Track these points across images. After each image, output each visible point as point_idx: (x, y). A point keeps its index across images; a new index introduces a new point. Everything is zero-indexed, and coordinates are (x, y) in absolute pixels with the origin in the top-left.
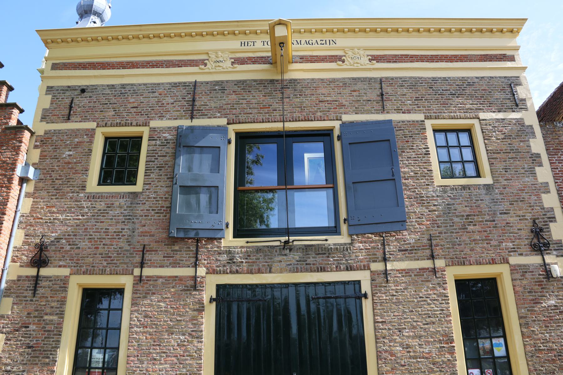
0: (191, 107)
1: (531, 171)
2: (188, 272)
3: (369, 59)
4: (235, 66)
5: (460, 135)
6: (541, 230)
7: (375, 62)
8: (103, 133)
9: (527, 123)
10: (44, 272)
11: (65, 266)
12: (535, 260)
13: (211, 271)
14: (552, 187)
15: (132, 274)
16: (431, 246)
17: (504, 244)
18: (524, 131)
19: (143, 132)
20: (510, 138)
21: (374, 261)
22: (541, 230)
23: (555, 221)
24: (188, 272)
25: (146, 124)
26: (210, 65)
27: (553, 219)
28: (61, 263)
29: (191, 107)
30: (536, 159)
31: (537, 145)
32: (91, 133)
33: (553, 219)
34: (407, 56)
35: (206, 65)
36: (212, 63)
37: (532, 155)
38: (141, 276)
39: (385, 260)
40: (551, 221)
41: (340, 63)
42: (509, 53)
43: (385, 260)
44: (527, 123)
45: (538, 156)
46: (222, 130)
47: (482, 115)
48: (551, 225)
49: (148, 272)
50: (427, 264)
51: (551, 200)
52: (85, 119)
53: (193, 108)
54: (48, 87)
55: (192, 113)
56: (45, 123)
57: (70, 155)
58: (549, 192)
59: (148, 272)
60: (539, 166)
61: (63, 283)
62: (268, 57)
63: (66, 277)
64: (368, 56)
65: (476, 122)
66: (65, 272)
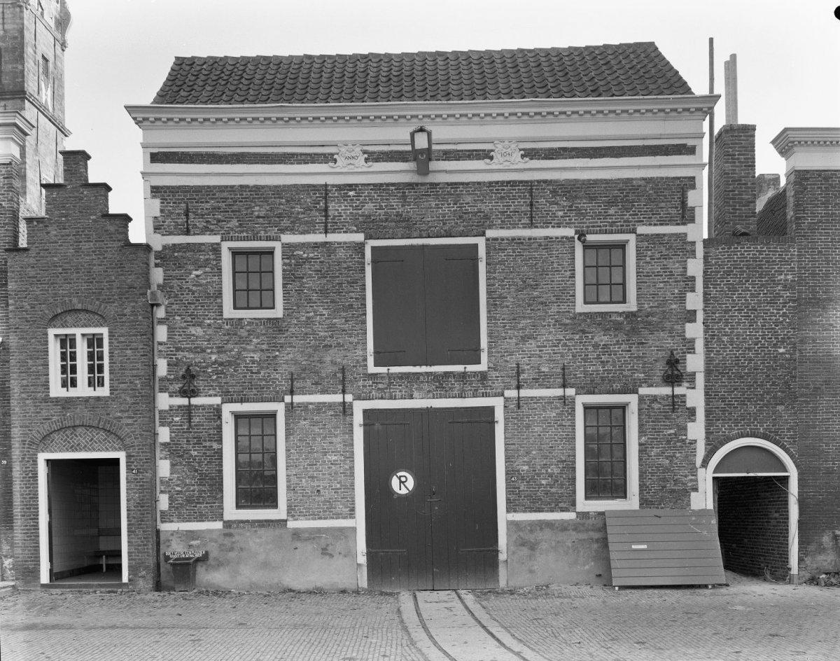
0: (324, 218)
1: (680, 297)
2: (338, 398)
3: (522, 155)
4: (370, 163)
5: (612, 253)
6: (677, 361)
7: (527, 159)
8: (230, 249)
9: (689, 239)
10: (195, 401)
11: (215, 395)
12: (666, 391)
13: (358, 398)
14: (700, 316)
15: (283, 401)
16: (564, 375)
17: (636, 375)
18: (684, 247)
19: (274, 248)
20: (666, 259)
21: (508, 389)
22: (677, 361)
23: (694, 353)
24: (338, 398)
25: (277, 239)
26: (341, 161)
27: (692, 350)
28: (211, 392)
29: (324, 218)
30: (689, 283)
31: (695, 267)
32: (216, 249)
33: (692, 350)
34: (565, 149)
35: (335, 161)
36: (343, 159)
37: (687, 278)
38: (292, 403)
39: (518, 387)
40: (690, 353)
41: (488, 161)
42: (690, 143)
43: (518, 387)
44: (689, 239)
45: (693, 279)
46: (360, 247)
47: (642, 230)
48: (689, 356)
49: (298, 399)
50: (559, 392)
51: (695, 330)
52: (205, 230)
53: (326, 219)
54: (153, 187)
55: (326, 226)
56: (159, 235)
57: (197, 276)
58: (694, 321)
59: (298, 399)
60: (691, 291)
61: (217, 412)
62: (406, 152)
63: (218, 405)
64: (520, 150)
65: (632, 238)
66: (217, 400)
